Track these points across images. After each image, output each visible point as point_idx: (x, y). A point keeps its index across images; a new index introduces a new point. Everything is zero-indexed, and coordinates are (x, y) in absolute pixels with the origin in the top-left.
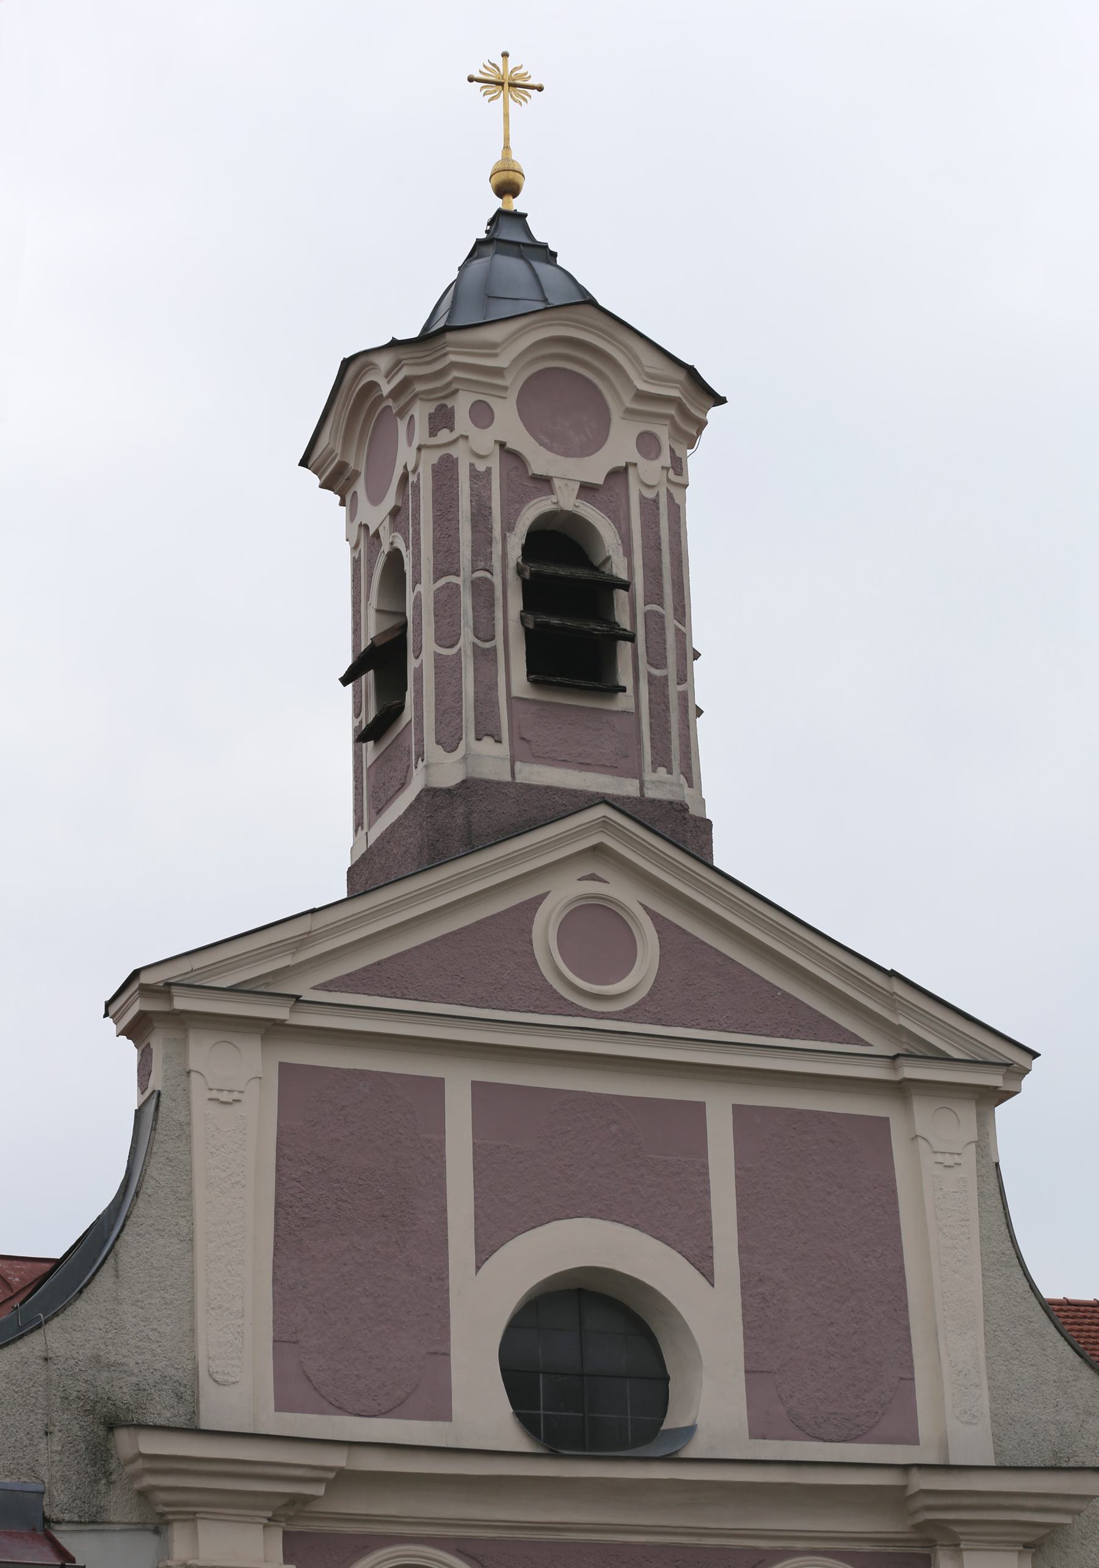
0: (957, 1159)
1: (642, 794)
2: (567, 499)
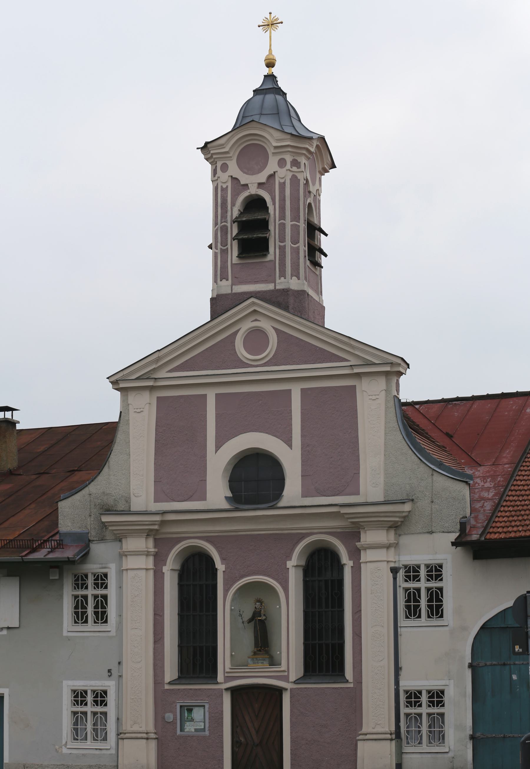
0: (377, 397)
1: (275, 288)
2: (253, 190)
